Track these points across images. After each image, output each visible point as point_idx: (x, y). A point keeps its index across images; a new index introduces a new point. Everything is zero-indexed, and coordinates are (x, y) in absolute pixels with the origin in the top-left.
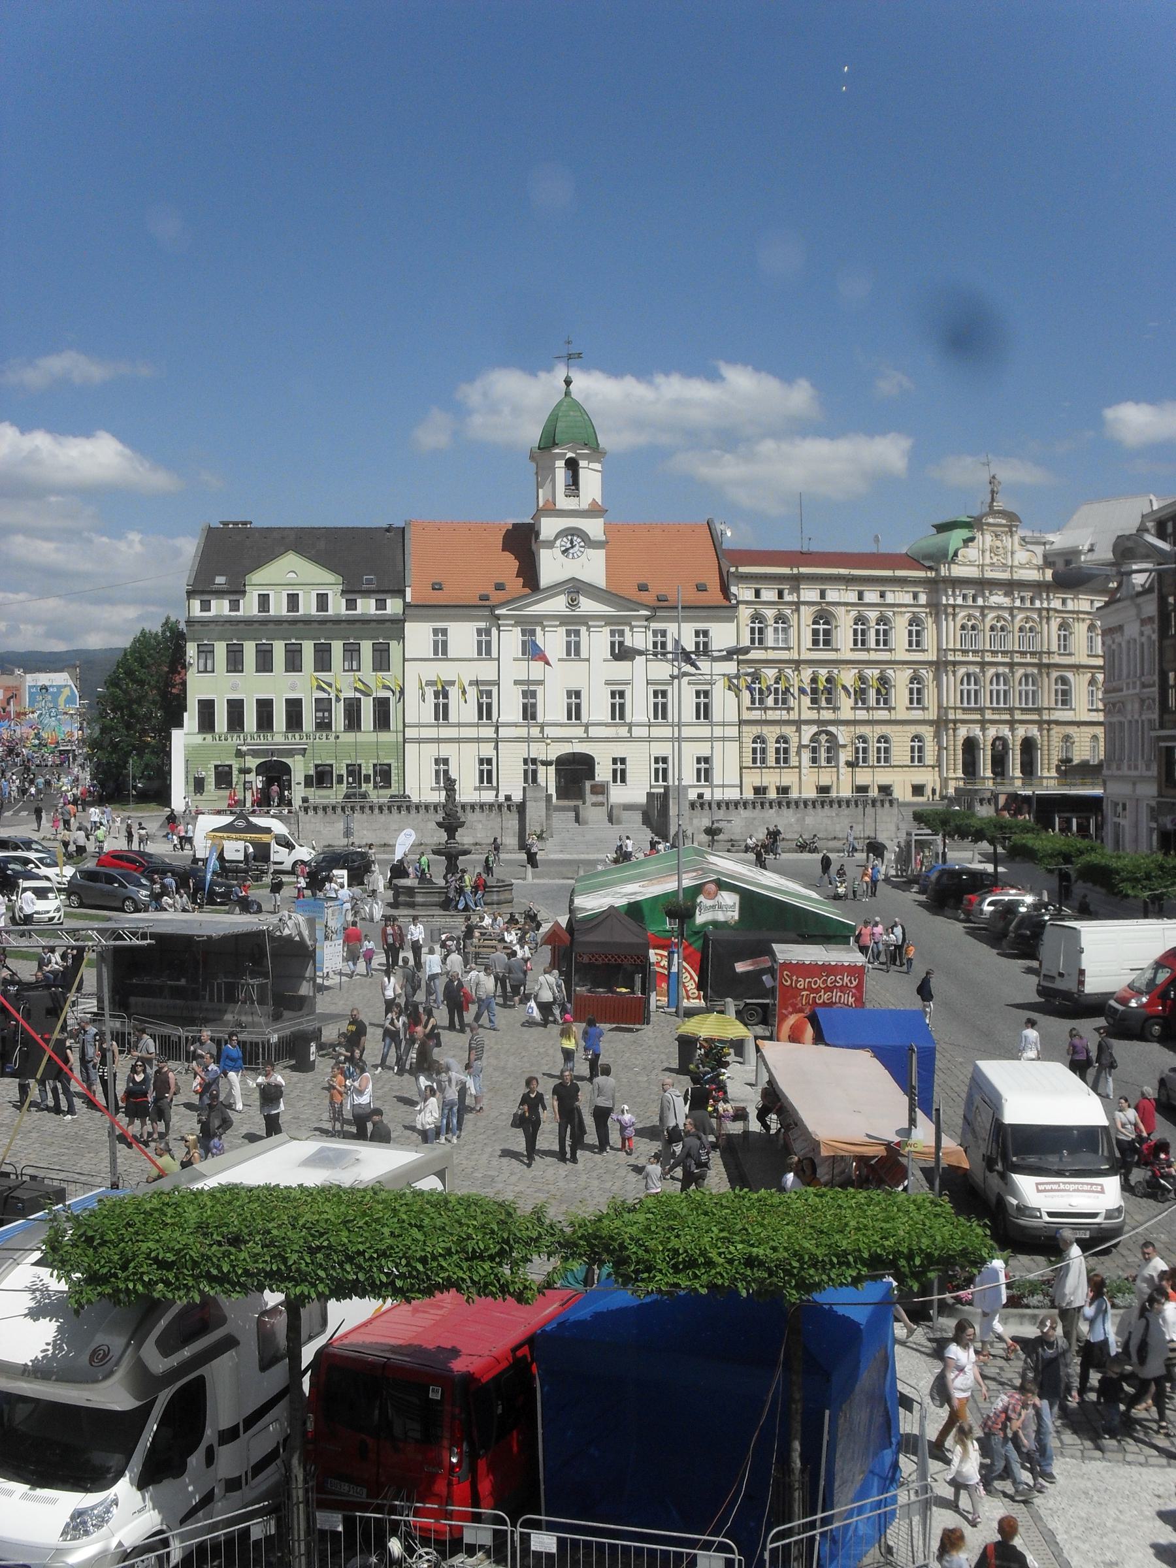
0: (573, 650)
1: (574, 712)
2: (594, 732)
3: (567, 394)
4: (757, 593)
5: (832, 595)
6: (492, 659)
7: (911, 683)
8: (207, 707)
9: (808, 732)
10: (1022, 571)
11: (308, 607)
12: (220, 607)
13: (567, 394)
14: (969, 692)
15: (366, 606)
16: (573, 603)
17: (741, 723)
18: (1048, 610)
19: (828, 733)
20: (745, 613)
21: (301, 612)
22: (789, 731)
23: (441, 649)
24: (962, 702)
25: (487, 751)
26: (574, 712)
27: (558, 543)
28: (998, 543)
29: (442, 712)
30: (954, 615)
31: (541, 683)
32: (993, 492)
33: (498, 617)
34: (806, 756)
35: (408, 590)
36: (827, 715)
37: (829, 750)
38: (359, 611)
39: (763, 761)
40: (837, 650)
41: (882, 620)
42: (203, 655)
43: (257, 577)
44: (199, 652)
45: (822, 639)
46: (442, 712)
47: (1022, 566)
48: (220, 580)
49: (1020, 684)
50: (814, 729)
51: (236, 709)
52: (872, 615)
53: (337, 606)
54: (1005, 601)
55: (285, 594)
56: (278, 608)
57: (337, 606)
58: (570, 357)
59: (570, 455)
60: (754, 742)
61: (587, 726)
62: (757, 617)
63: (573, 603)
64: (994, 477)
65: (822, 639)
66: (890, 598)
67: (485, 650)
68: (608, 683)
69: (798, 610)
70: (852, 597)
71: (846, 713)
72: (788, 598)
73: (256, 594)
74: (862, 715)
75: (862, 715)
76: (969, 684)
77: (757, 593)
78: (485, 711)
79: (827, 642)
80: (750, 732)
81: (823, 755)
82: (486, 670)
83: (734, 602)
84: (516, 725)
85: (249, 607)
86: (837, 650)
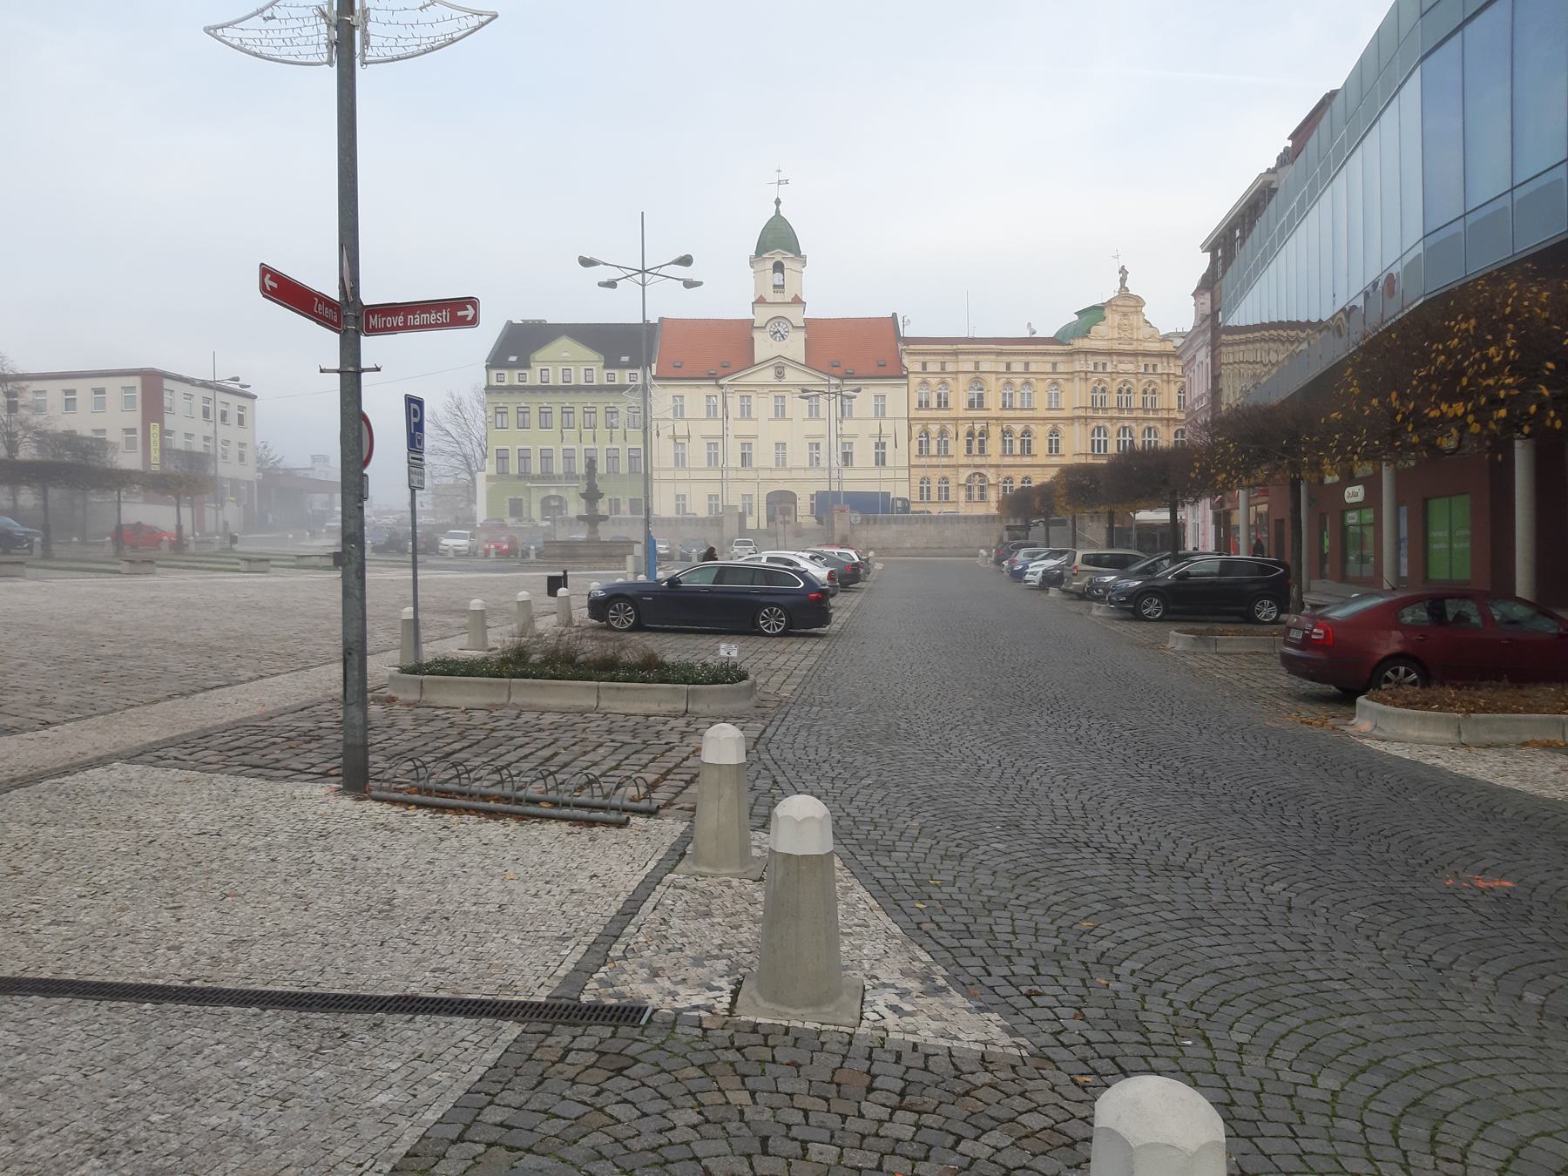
0: (780, 413)
1: (781, 462)
2: (795, 474)
3: (778, 211)
4: (924, 365)
5: (984, 367)
6: (717, 419)
7: (1051, 435)
8: (502, 457)
9: (964, 475)
10: (1146, 344)
11: (578, 378)
12: (511, 377)
13: (778, 211)
14: (1099, 441)
15: (622, 377)
16: (780, 374)
17: (910, 467)
18: (1168, 374)
19: (981, 475)
20: (914, 380)
21: (573, 383)
22: (947, 473)
23: (679, 412)
24: (1093, 450)
25: (715, 489)
26: (781, 462)
27: (768, 327)
28: (1126, 322)
29: (680, 461)
30: (1087, 379)
31: (756, 437)
32: (1123, 280)
33: (721, 387)
34: (963, 494)
35: (654, 366)
36: (978, 461)
37: (982, 489)
38: (617, 383)
39: (929, 497)
40: (988, 409)
41: (1027, 383)
42: (499, 416)
43: (539, 355)
44: (496, 413)
45: (977, 403)
46: (680, 461)
47: (1146, 340)
48: (513, 359)
49: (1144, 436)
50: (970, 471)
51: (524, 457)
52: (1018, 381)
53: (600, 376)
54: (1130, 367)
55: (560, 368)
56: (556, 379)
57: (600, 376)
58: (779, 182)
59: (778, 258)
60: (922, 483)
61: (791, 469)
62: (924, 382)
63: (780, 374)
64: (1123, 267)
65: (977, 403)
66: (1033, 368)
67: (711, 413)
68: (807, 437)
69: (957, 379)
70: (1003, 368)
71: (994, 460)
72: (950, 367)
73: (538, 369)
74: (1008, 461)
75: (1008, 461)
76: (1099, 435)
77: (924, 365)
78: (712, 459)
79: (981, 406)
80: (918, 474)
81: (976, 493)
82: (714, 428)
83: (905, 373)
84: (737, 469)
85: (533, 377)
86: (988, 409)
